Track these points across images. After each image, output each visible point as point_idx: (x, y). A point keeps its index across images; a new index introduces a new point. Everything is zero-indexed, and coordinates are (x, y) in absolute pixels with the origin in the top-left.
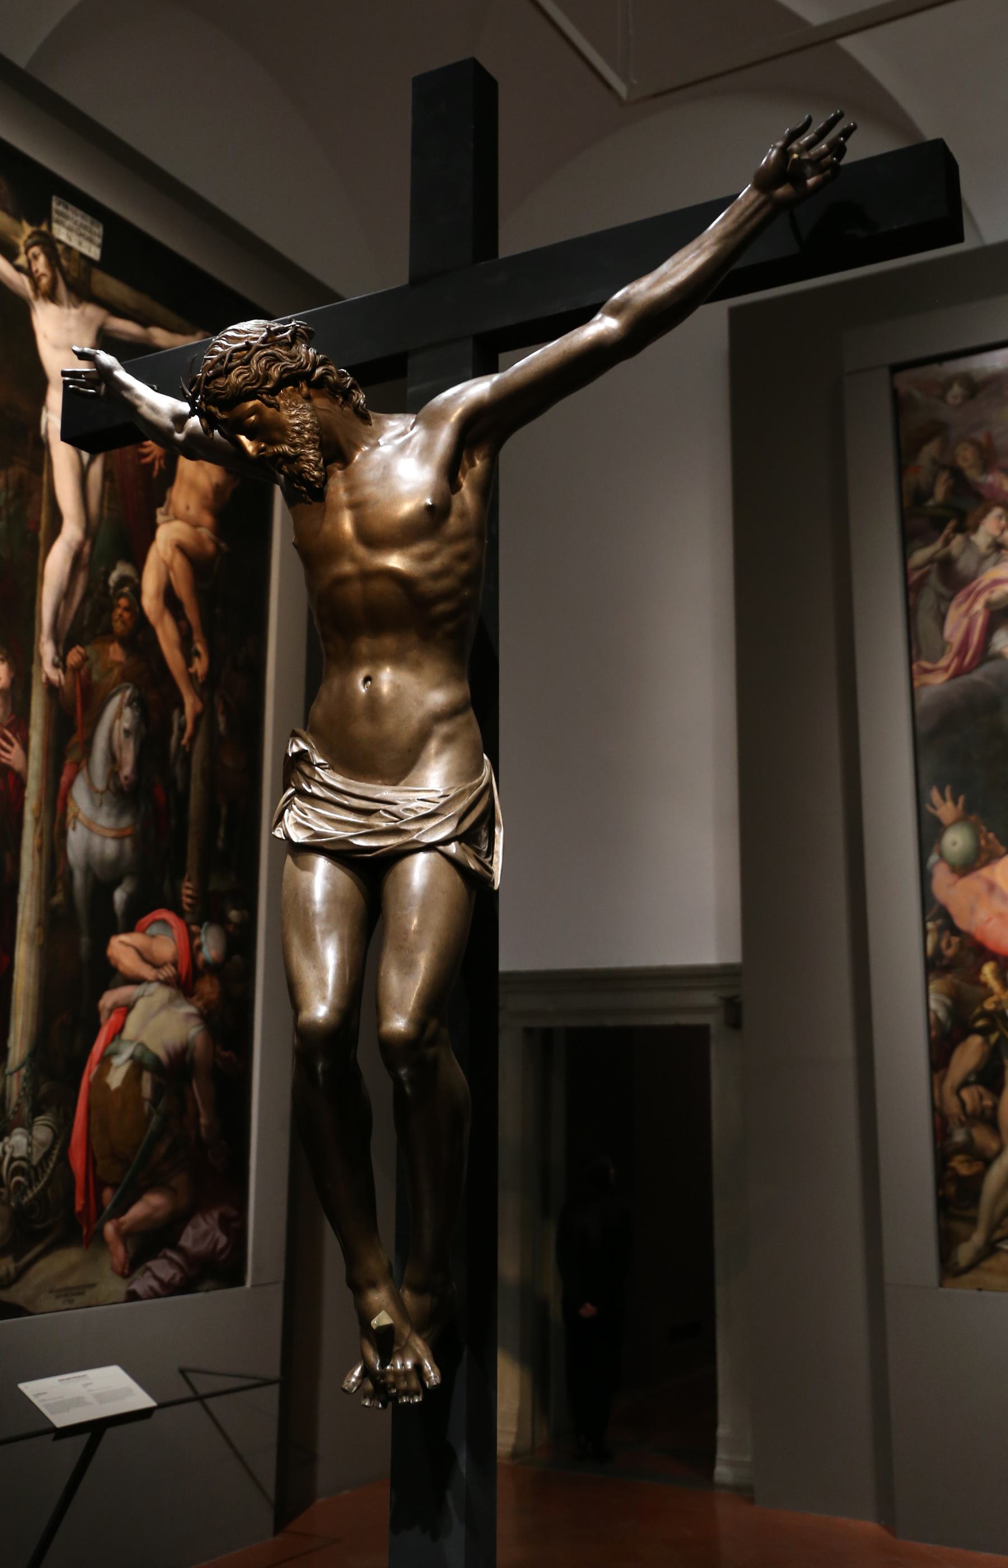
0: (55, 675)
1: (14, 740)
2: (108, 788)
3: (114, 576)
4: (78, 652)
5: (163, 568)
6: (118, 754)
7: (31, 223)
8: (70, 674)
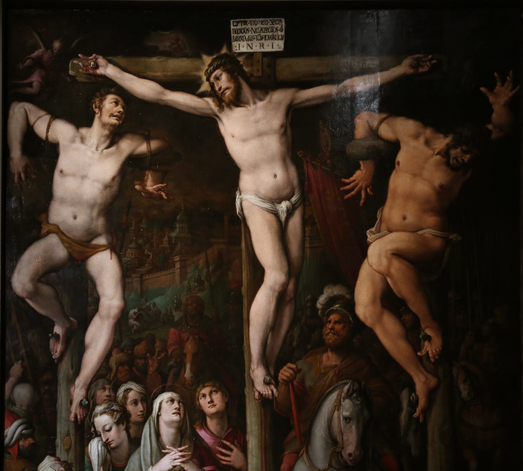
0: (266, 391)
1: (232, 447)
2: (330, 465)
3: (322, 299)
4: (289, 368)
6: (339, 438)
7: (209, 54)
8: (282, 388)
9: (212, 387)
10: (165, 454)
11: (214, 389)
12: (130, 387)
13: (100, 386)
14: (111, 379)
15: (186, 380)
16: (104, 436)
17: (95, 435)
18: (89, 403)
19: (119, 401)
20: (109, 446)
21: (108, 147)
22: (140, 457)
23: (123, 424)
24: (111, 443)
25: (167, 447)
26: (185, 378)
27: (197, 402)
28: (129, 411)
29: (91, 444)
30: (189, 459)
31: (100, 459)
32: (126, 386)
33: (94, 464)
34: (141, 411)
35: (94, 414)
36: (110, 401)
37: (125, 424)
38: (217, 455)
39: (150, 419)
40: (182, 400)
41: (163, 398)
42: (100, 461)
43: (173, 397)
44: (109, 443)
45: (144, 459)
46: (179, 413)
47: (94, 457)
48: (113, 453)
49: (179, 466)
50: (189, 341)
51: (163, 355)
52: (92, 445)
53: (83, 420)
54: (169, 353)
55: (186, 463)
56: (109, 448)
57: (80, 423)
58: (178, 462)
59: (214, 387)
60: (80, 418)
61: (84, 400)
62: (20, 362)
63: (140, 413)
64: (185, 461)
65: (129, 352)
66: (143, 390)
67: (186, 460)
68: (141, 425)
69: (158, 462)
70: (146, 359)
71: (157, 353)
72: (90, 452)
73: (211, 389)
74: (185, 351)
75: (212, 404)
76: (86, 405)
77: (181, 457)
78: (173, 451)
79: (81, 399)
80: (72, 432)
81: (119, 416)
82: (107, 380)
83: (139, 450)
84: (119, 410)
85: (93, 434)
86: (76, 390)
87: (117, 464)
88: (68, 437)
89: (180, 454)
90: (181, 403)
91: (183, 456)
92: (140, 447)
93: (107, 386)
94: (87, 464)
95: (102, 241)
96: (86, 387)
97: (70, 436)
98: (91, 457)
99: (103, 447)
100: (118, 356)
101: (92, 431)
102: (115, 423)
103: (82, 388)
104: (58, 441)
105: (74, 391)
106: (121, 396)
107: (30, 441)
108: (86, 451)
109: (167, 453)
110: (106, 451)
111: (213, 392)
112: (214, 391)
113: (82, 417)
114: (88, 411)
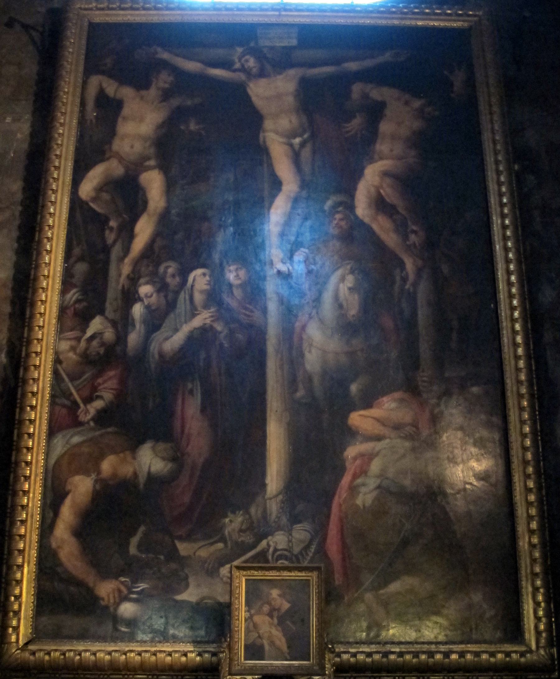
5: (373, 190)
21: (161, 102)
68: (177, 293)
89: (210, 314)
95: (152, 163)
107: (85, 304)
109: (198, 314)
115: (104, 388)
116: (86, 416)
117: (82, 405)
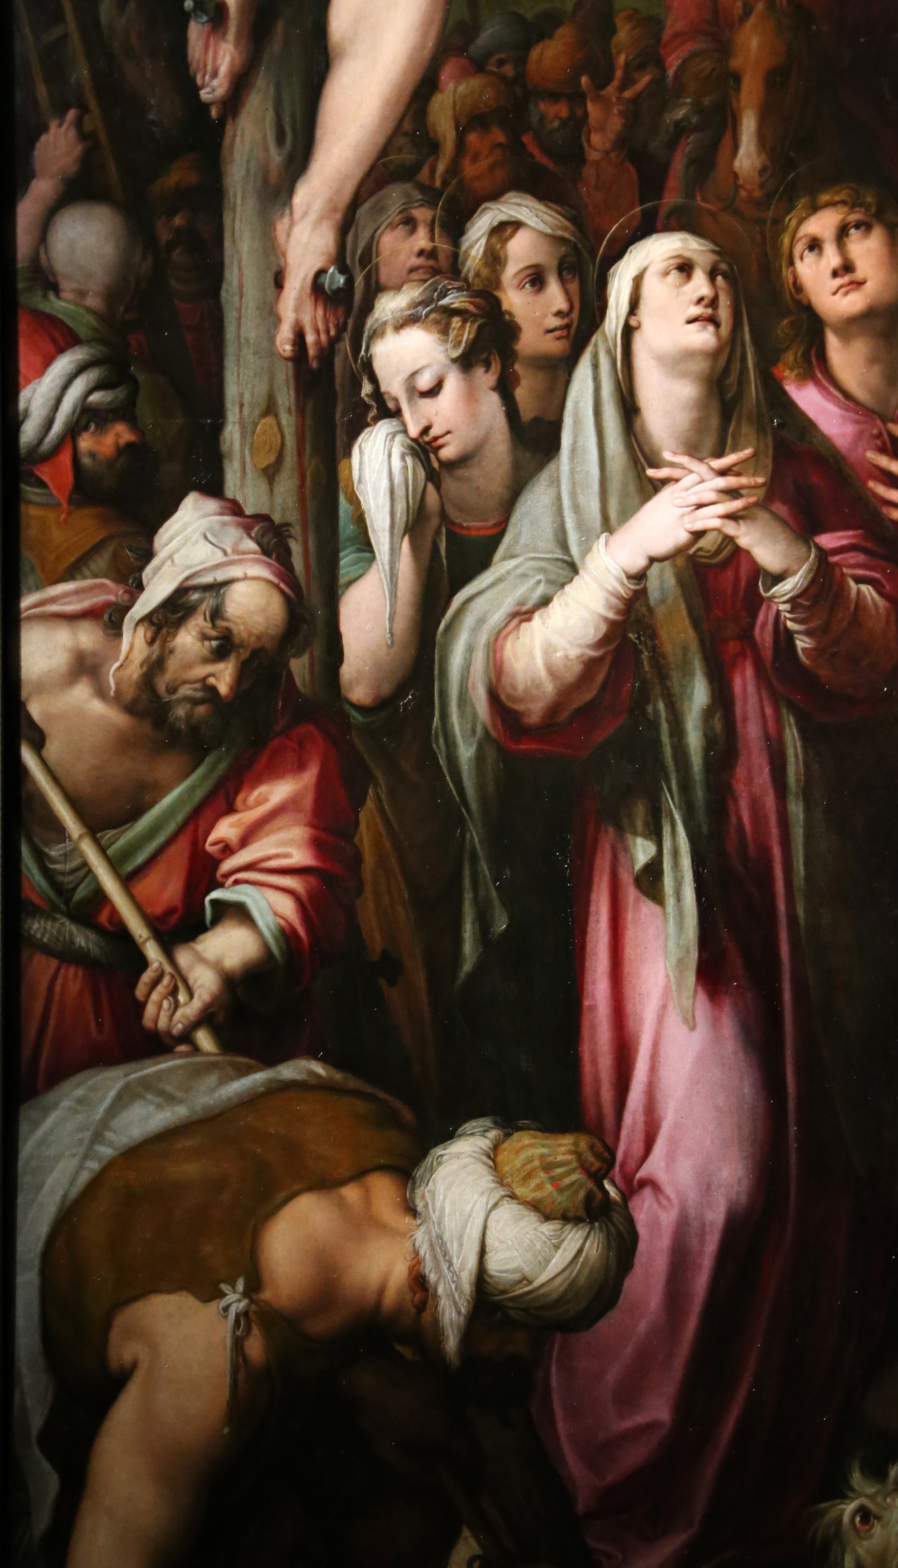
9: (845, 209)
10: (658, 486)
11: (854, 217)
12: (513, 213)
13: (393, 212)
14: (438, 183)
15: (741, 182)
16: (412, 414)
17: (375, 411)
18: (350, 282)
19: (471, 275)
20: (432, 456)
22: (559, 498)
23: (488, 366)
24: (441, 441)
25: (667, 456)
26: (736, 176)
27: (787, 274)
28: (510, 314)
29: (363, 445)
30: (756, 505)
31: (401, 507)
32: (499, 209)
33: (376, 528)
34: (559, 314)
35: (372, 326)
36: (435, 272)
37: (496, 366)
38: (871, 484)
39: (596, 345)
40: (723, 266)
41: (647, 256)
42: (398, 515)
43: (687, 254)
44: (434, 444)
45: (576, 508)
46: (713, 320)
47: (375, 498)
48: (450, 484)
49: (715, 533)
50: (753, 19)
51: (645, 80)
52: (366, 452)
53: (327, 353)
54: (671, 72)
55: (743, 518)
56: (436, 465)
57: (314, 364)
58: (713, 517)
59: (857, 209)
60: (318, 342)
61: (331, 270)
62: (71, 114)
63: (555, 322)
64: (741, 513)
65: (509, 70)
66: (565, 229)
67: (745, 508)
69: (631, 516)
70: (577, 98)
71: (619, 73)
72: (360, 481)
73: (842, 216)
74: (735, 63)
75: (846, 279)
76: (339, 290)
77: (723, 497)
78: (691, 472)
79: (318, 265)
80: (286, 398)
81: (469, 332)
82: (421, 187)
83: (553, 470)
84: (471, 308)
85: (368, 408)
86: (296, 230)
87: (468, 528)
88: (269, 420)
90: (719, 278)
91: (732, 493)
92: (559, 459)
93: (422, 214)
94: (346, 527)
96: (338, 216)
97: (276, 416)
98: (361, 498)
99: (409, 460)
100: (461, 88)
101: (363, 394)
102: (454, 361)
103: (320, 219)
104: (232, 434)
105: (288, 235)
106: (478, 250)
108: (342, 474)
109: (665, 482)
110: (422, 474)
111: (852, 231)
112: (857, 226)
113: (323, 337)
114: (347, 316)
115: (250, 867)
116: (176, 1005)
117: (152, 951)
